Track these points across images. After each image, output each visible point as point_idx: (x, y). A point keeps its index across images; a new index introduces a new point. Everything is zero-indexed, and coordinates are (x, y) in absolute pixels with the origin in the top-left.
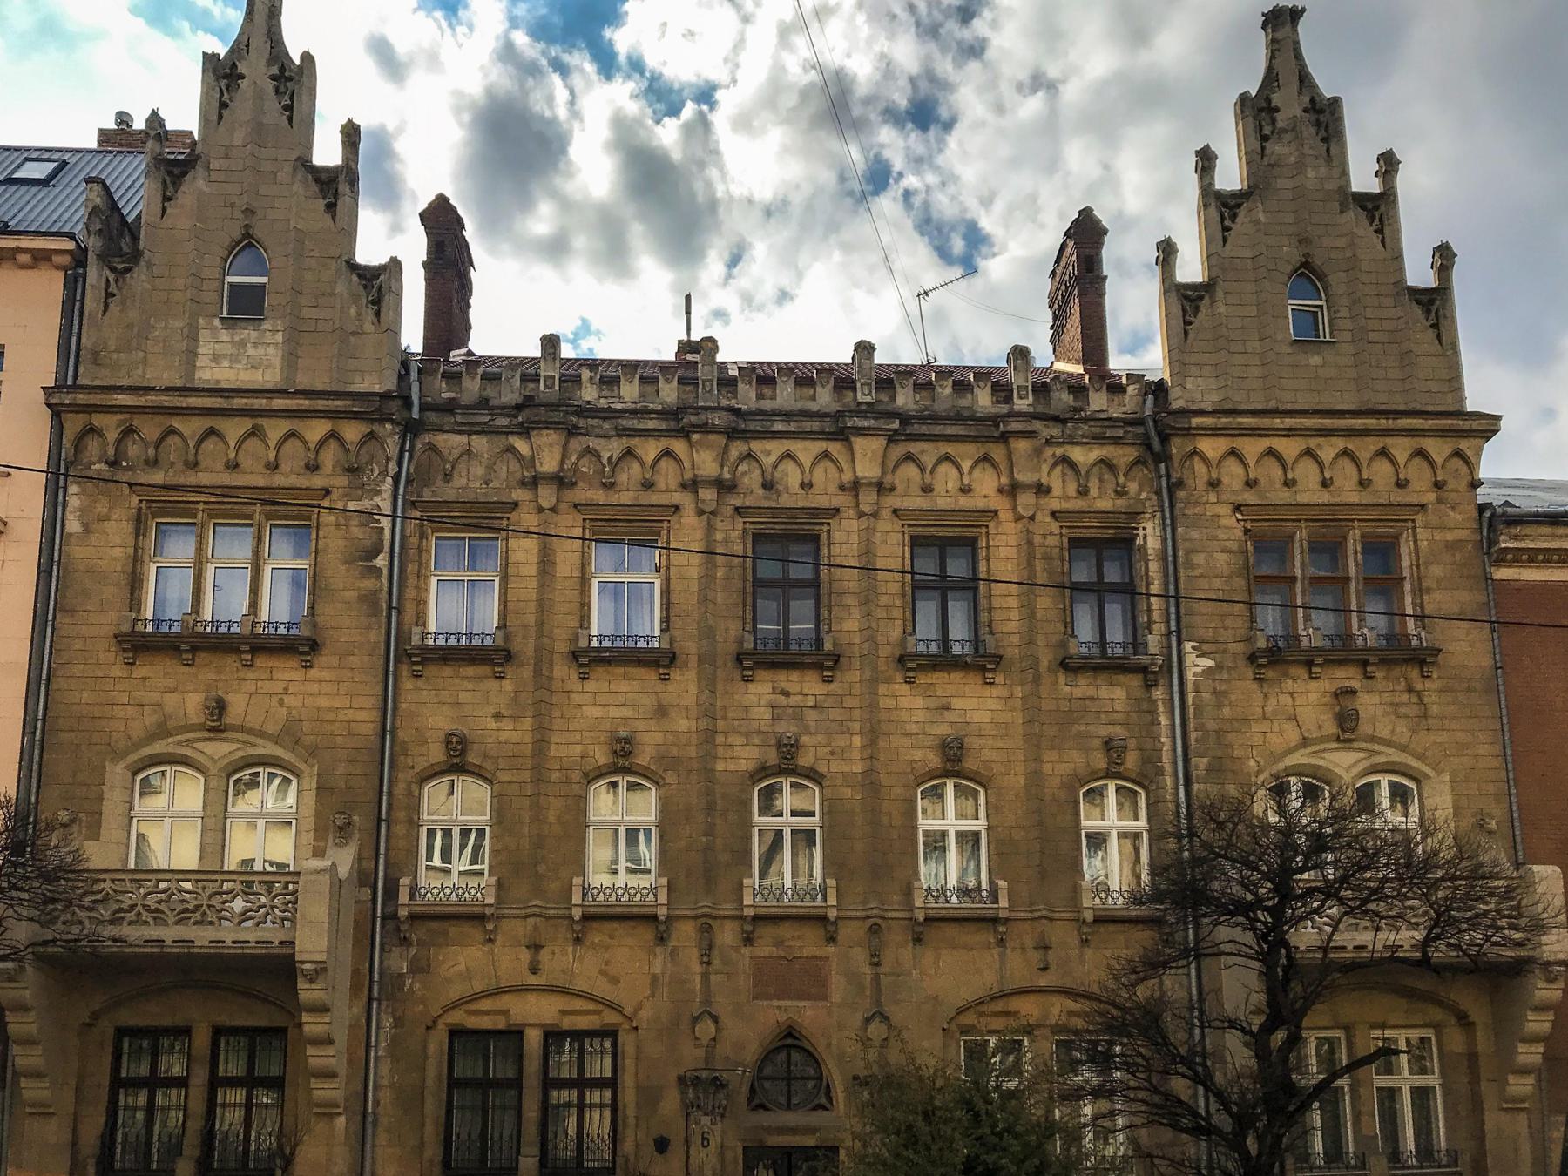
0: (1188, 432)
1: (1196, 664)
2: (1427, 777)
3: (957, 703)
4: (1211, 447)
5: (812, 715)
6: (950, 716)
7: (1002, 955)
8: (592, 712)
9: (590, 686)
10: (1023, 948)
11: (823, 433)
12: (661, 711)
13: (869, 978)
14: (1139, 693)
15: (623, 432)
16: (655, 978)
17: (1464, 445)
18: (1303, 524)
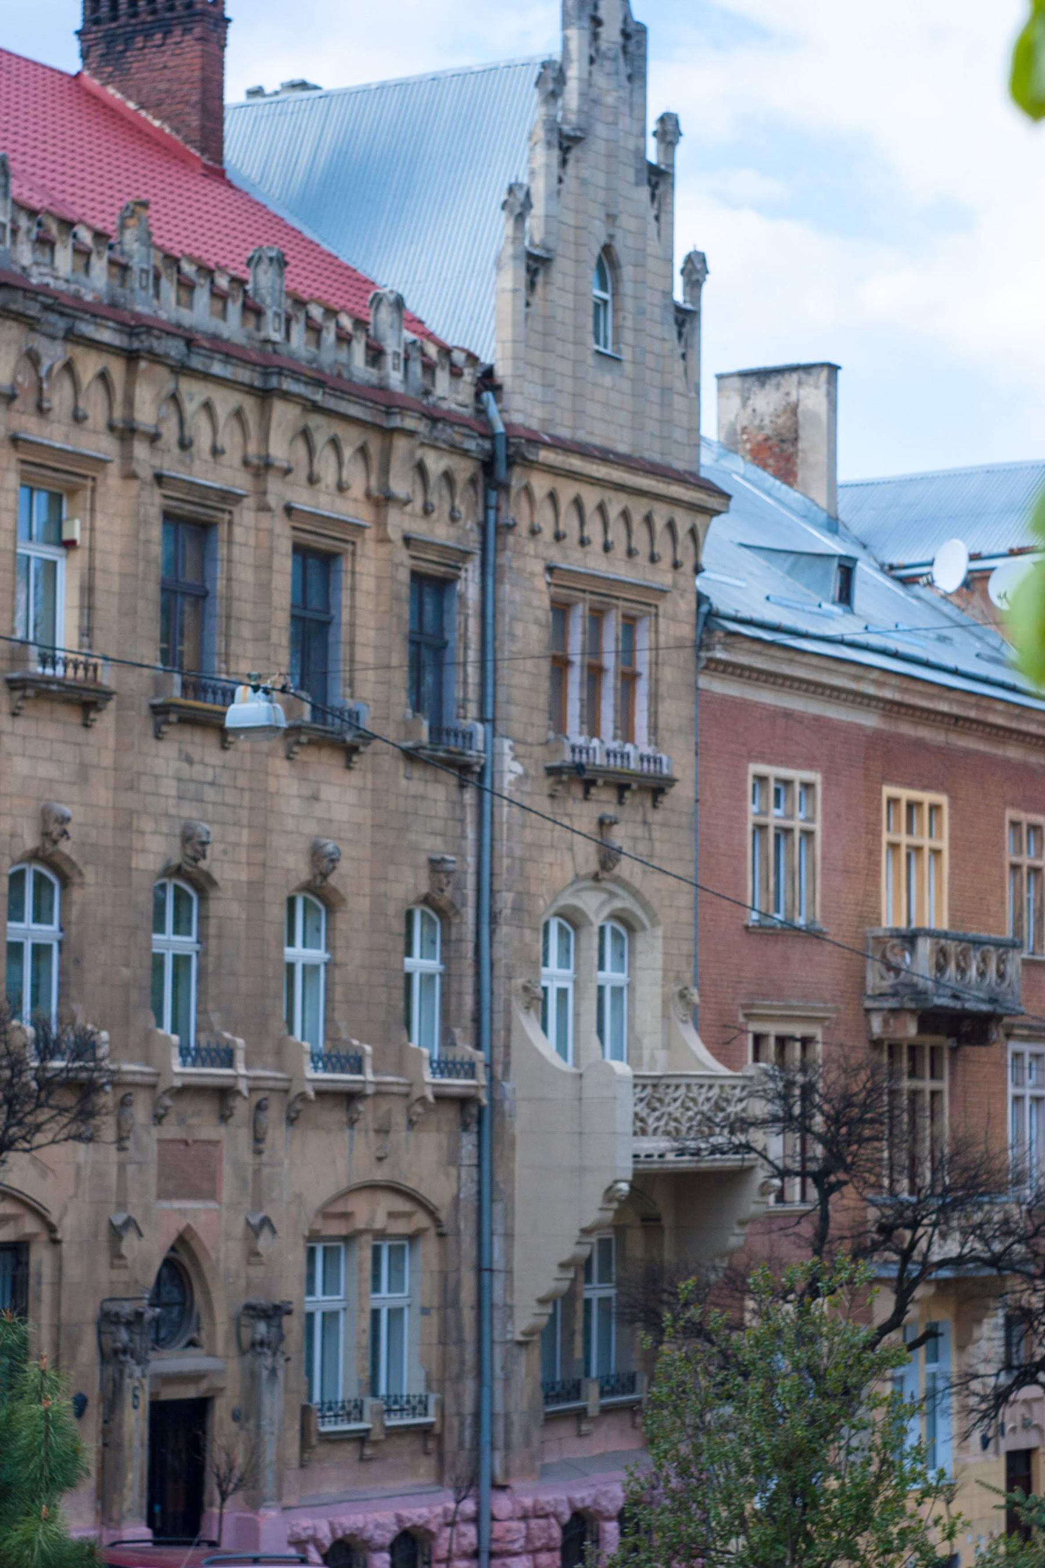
0: (531, 465)
1: (510, 770)
2: (644, 928)
3: (328, 793)
4: (541, 485)
5: (210, 794)
6: (319, 810)
7: (351, 1138)
8: (21, 766)
9: (21, 726)
10: (366, 1131)
11: (252, 387)
12: (83, 773)
13: (250, 1169)
14: (454, 795)
15: (72, 337)
16: (78, 1168)
17: (700, 520)
18: (588, 596)
